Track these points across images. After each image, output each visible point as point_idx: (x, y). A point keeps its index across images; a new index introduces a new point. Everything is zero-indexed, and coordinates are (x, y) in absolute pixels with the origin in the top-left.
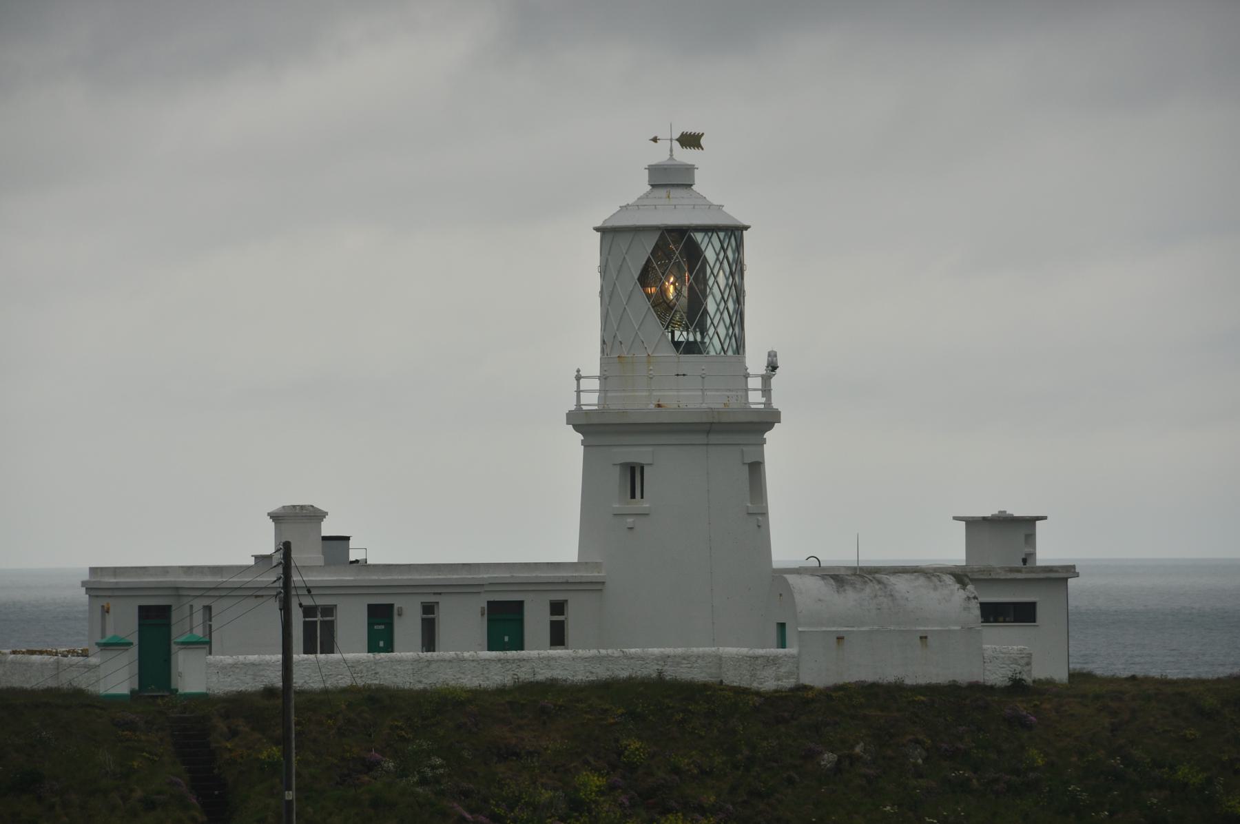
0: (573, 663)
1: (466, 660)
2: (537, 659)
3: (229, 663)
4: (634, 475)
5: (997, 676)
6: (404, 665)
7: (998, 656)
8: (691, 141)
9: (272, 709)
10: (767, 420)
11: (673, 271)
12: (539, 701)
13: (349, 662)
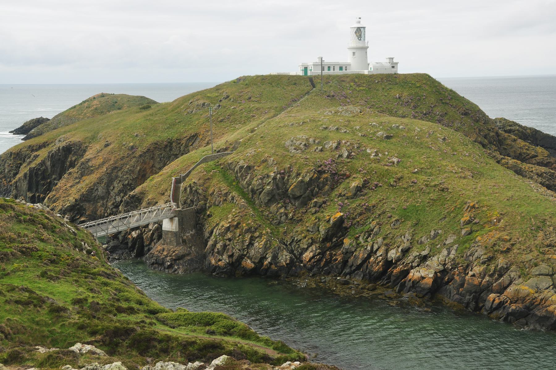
1: (337, 72)
2: (344, 72)
3: (313, 71)
4: (354, 53)
5: (393, 73)
6: (331, 72)
7: (392, 71)
8: (360, 18)
9: (317, 77)
10: (368, 47)
11: (359, 32)
12: (347, 76)
13: (326, 72)
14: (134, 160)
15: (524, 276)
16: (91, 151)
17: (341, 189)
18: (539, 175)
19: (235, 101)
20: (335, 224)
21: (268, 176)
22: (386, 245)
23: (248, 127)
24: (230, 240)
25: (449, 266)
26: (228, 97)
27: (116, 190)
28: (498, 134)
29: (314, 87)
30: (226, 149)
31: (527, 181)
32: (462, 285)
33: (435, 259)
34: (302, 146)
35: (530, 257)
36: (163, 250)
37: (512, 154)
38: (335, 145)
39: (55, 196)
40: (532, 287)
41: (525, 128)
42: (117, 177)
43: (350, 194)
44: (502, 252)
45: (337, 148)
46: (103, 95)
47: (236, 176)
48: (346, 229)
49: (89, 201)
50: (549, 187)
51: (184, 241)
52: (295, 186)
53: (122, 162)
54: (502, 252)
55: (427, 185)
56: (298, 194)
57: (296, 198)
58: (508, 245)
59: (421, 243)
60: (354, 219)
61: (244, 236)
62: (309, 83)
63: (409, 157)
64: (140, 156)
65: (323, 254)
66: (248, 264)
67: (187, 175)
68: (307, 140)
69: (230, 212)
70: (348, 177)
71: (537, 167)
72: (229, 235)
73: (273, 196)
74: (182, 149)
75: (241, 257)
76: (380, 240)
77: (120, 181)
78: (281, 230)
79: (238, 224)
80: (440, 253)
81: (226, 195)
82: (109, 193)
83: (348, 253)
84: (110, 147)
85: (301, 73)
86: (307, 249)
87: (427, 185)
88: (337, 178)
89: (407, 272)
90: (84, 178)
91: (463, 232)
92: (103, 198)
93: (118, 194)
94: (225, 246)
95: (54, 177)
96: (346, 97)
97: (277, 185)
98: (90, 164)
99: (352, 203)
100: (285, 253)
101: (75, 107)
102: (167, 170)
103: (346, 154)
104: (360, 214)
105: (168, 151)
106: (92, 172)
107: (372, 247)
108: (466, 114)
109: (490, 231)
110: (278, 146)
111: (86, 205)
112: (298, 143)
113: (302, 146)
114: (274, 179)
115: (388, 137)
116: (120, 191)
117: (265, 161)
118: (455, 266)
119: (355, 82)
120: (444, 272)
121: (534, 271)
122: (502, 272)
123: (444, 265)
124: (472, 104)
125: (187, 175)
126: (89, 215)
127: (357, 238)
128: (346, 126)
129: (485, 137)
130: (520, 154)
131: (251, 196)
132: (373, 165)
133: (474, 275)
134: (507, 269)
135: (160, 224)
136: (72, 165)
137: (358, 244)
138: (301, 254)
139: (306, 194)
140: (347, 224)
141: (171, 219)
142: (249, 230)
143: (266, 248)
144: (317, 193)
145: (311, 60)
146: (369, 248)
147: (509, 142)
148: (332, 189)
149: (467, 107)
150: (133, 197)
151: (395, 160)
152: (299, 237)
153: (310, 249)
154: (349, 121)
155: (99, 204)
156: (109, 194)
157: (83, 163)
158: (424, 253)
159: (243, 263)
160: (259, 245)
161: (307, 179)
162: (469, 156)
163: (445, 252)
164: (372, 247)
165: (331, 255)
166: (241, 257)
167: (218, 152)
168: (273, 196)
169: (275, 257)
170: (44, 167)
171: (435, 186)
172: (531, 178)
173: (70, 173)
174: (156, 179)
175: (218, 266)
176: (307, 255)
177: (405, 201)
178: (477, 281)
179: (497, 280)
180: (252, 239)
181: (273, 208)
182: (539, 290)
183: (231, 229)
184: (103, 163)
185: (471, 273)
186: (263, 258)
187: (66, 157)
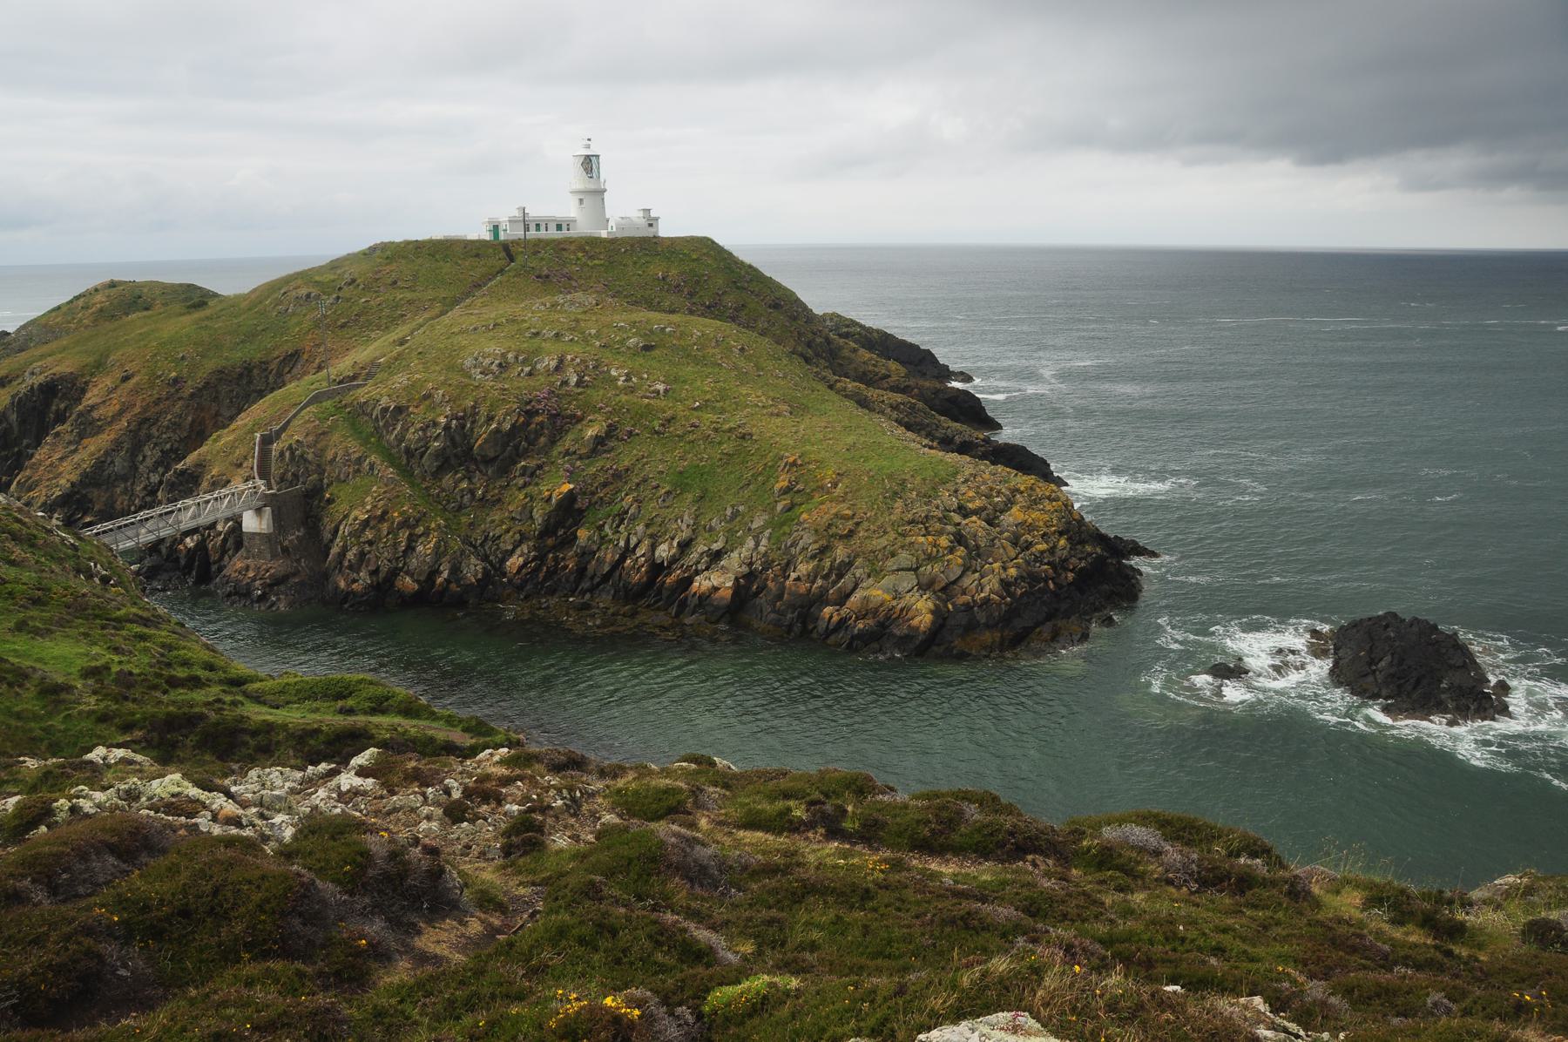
0: (573, 233)
1: (553, 233)
2: (564, 233)
3: (509, 233)
6: (542, 234)
7: (649, 233)
9: (516, 242)
11: (589, 164)
12: (570, 241)
13: (532, 234)
14: (180, 403)
15: (876, 573)
16: (96, 391)
17: (568, 442)
18: (895, 407)
19: (367, 288)
20: (560, 503)
21: (435, 424)
22: (651, 536)
23: (395, 335)
24: (370, 543)
25: (758, 566)
26: (353, 281)
27: (149, 462)
28: (828, 341)
29: (512, 260)
30: (354, 378)
31: (877, 418)
32: (780, 597)
33: (735, 555)
34: (494, 367)
35: (883, 542)
36: (247, 568)
37: (852, 373)
38: (553, 364)
40: (887, 591)
41: (870, 330)
42: (149, 437)
43: (583, 451)
44: (841, 537)
45: (557, 368)
46: (113, 285)
47: (376, 425)
48: (581, 511)
49: (97, 485)
50: (908, 427)
51: (285, 550)
52: (486, 441)
53: (157, 409)
54: (841, 537)
55: (716, 430)
56: (491, 454)
57: (488, 461)
58: (850, 524)
59: (711, 529)
60: (593, 494)
61: (396, 537)
62: (503, 254)
63: (685, 382)
64: (192, 395)
65: (541, 558)
66: (408, 583)
67: (284, 429)
68: (504, 355)
69: (367, 493)
70: (580, 420)
71: (891, 394)
72: (369, 535)
73: (447, 460)
74: (271, 379)
75: (394, 573)
76: (640, 528)
78: (464, 519)
79: (385, 513)
80: (742, 544)
81: (359, 461)
83: (586, 554)
84: (133, 381)
85: (487, 236)
86: (512, 552)
87: (716, 430)
88: (561, 422)
89: (690, 581)
90: (85, 442)
91: (779, 507)
92: (124, 478)
93: (154, 469)
94: (362, 555)
95: (25, 442)
96: (570, 279)
97: (452, 440)
98: (95, 414)
99: (588, 465)
100: (473, 560)
101: (59, 308)
102: (244, 420)
103: (574, 379)
104: (605, 485)
105: (244, 384)
106: (100, 430)
107: (628, 541)
108: (776, 306)
109: (822, 503)
110: (451, 368)
111: (94, 493)
112: (487, 361)
113: (494, 367)
114: (447, 428)
115: (647, 348)
116: (157, 464)
117: (428, 397)
118: (768, 565)
119: (584, 251)
120: (751, 576)
121: (891, 564)
122: (842, 569)
123: (751, 564)
124: (786, 289)
125: (284, 429)
127: (601, 528)
128: (572, 329)
129: (809, 345)
130: (864, 373)
131: (406, 460)
132: (624, 398)
133: (798, 579)
134: (850, 564)
135: (237, 521)
136: (61, 418)
137: (602, 538)
138: (503, 561)
139: (506, 454)
140: (581, 503)
141: (259, 511)
142: (405, 524)
143: (438, 553)
144: (526, 450)
145: (505, 213)
146: (622, 543)
147: (846, 353)
148: (553, 442)
149: (777, 294)
150: (183, 472)
151: (661, 387)
152: (498, 532)
153: (518, 551)
154: (577, 321)
156: (137, 469)
157: (80, 414)
158: (715, 547)
159: (399, 584)
160: (425, 549)
161: (507, 426)
162: (785, 377)
163: (750, 543)
164: (628, 541)
165: (556, 559)
166: (394, 573)
167: (341, 382)
168: (447, 460)
169: (455, 570)
171: (730, 430)
172: (882, 412)
173: (57, 434)
174: (225, 437)
175: (353, 592)
176: (514, 562)
177: (681, 458)
178: (803, 588)
179: (835, 583)
180: (412, 539)
181: (447, 480)
182: (897, 596)
183: (372, 523)
184: (121, 413)
185: (793, 575)
186: (435, 572)
187: (48, 405)
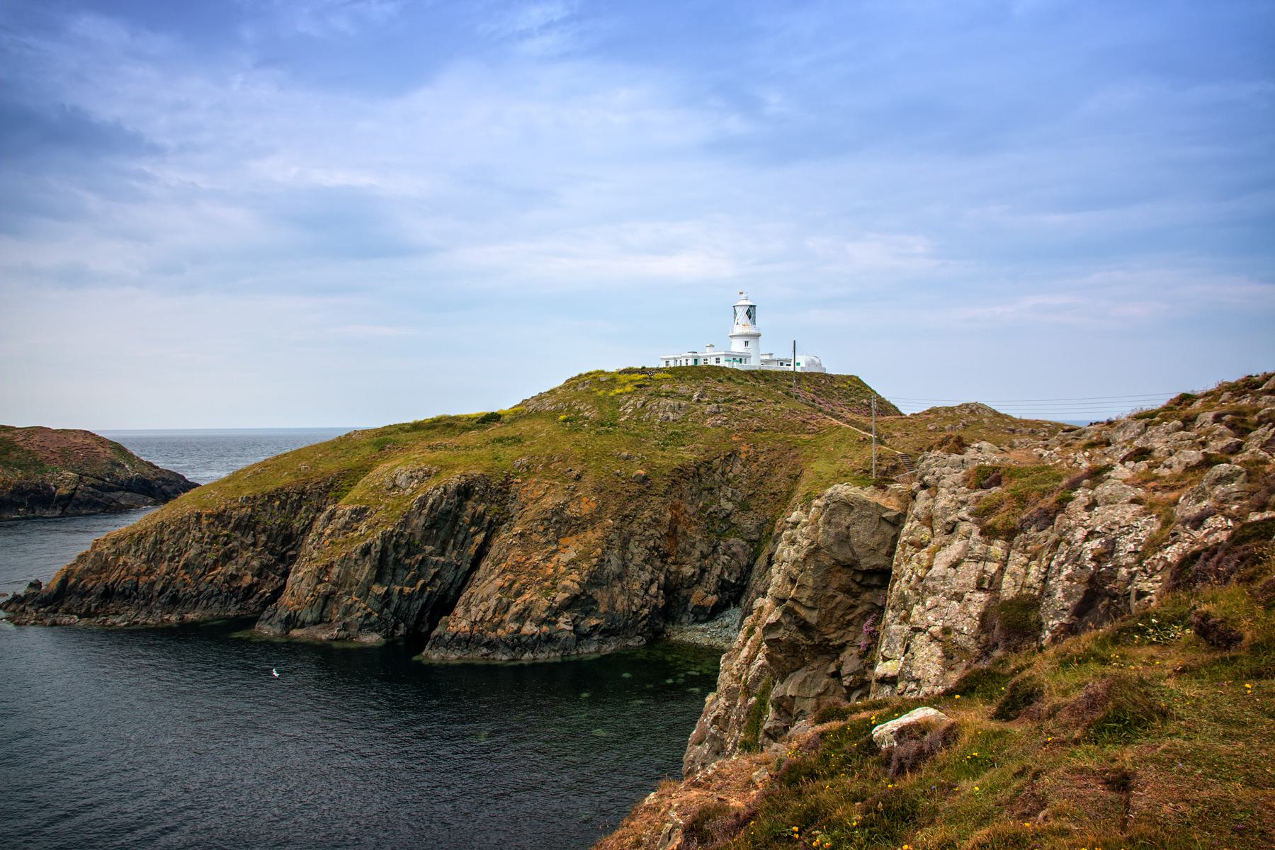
4: (747, 343)
27: (638, 560)
39: (514, 582)
42: (632, 534)
49: (599, 585)
77: (640, 542)
82: (625, 566)
111: (599, 594)
126: (605, 612)
155: (617, 590)
170: (409, 530)
187: (460, 506)
